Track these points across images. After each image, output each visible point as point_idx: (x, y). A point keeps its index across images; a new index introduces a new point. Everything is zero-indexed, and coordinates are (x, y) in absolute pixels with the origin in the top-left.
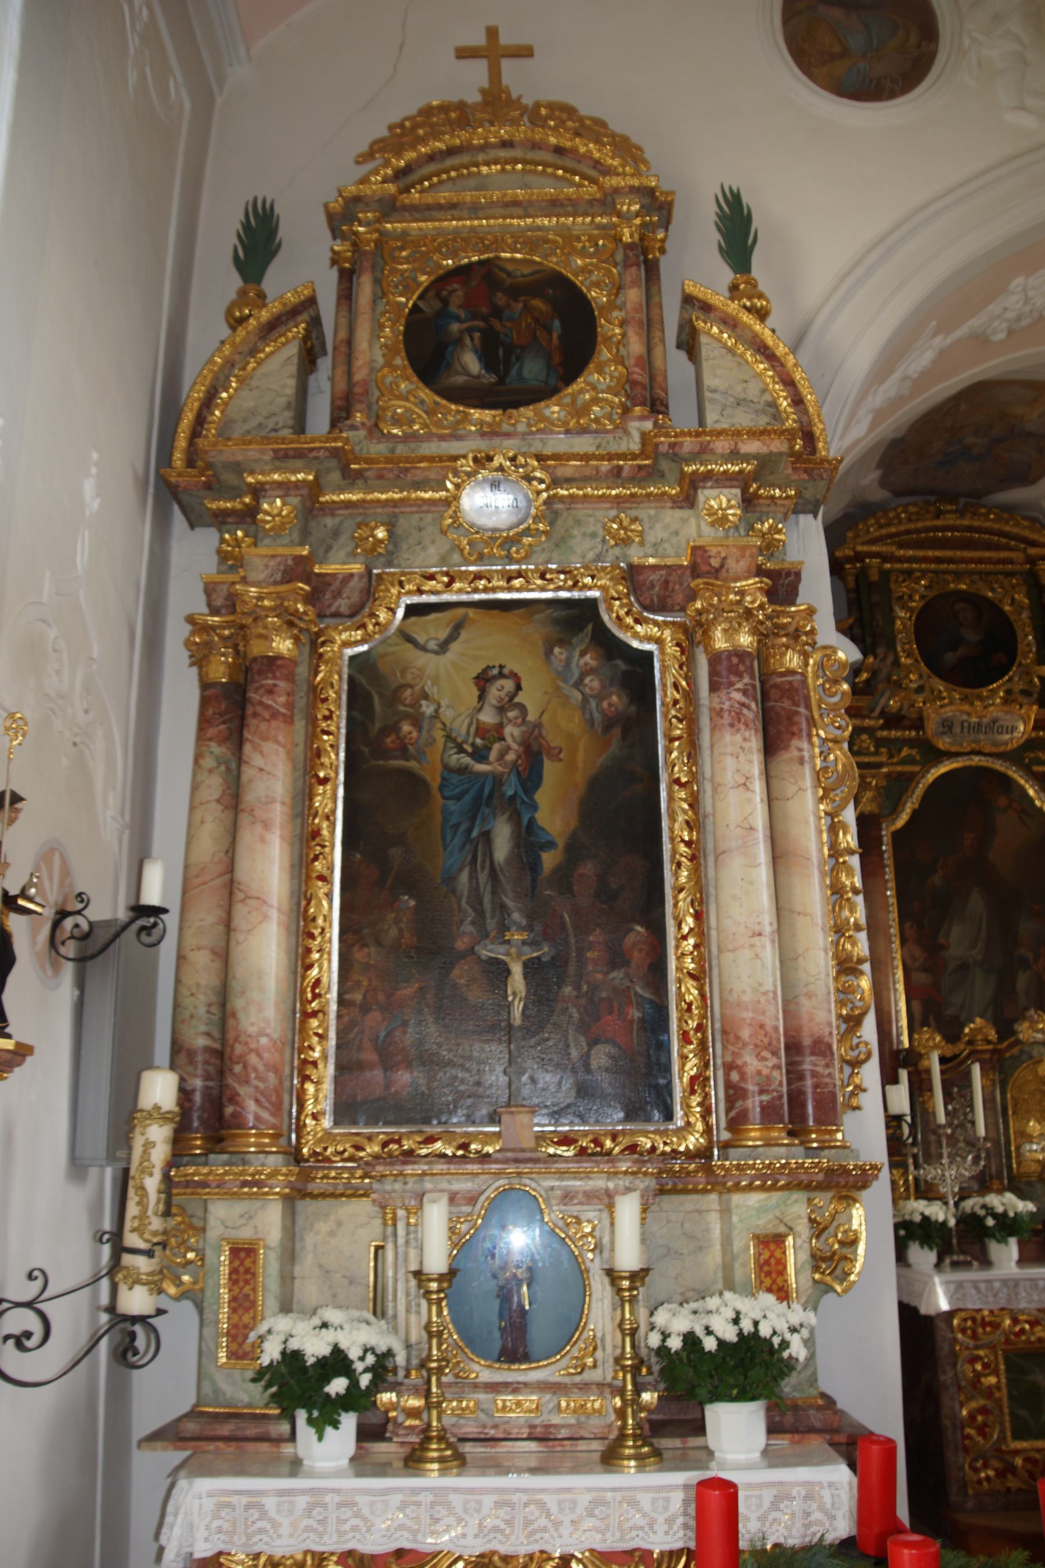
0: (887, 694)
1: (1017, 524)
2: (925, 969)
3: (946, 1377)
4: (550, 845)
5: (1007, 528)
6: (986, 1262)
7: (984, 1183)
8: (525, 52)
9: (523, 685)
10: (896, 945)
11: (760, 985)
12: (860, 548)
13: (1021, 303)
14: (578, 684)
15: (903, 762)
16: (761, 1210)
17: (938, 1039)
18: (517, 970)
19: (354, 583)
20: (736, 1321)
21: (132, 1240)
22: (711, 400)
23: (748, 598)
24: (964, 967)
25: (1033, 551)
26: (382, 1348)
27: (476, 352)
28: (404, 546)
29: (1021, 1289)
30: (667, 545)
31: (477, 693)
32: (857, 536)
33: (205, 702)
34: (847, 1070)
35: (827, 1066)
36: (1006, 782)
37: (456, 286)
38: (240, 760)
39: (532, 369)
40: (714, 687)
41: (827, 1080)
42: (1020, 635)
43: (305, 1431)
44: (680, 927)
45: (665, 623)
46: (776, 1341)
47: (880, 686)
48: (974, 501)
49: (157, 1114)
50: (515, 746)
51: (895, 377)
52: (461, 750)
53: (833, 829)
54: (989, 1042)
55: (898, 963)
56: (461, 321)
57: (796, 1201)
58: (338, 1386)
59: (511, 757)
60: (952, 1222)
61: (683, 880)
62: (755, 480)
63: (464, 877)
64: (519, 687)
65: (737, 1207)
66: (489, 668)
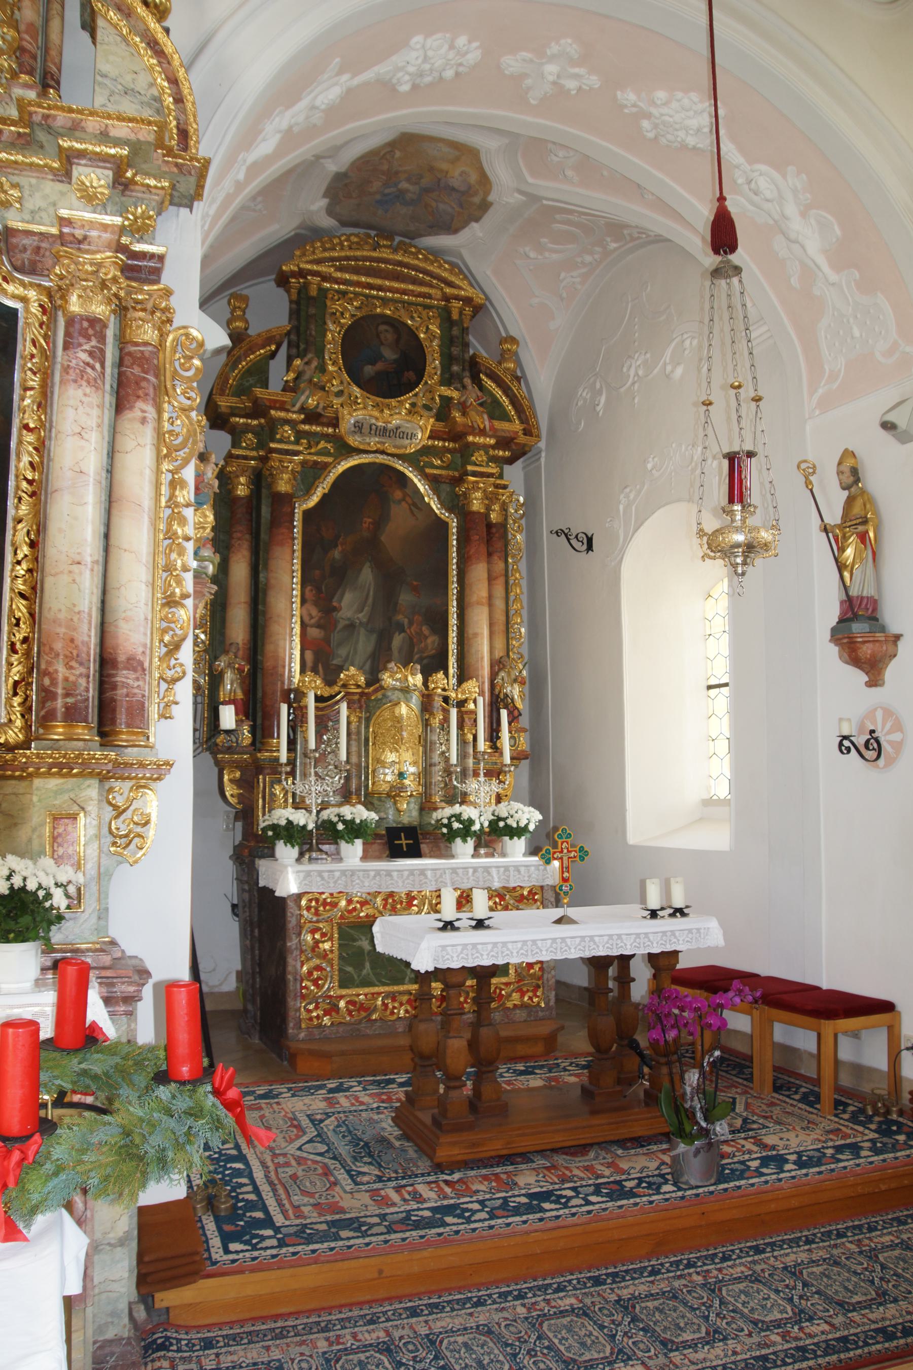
0: (307, 393)
1: (440, 266)
2: (319, 626)
3: (292, 943)
5: (430, 268)
6: (337, 857)
7: (346, 796)
10: (296, 606)
11: (74, 605)
12: (302, 266)
13: (420, 61)
15: (317, 454)
16: (58, 792)
17: (318, 682)
20: (9, 878)
23: (103, 270)
24: (351, 627)
25: (448, 290)
29: (355, 877)
30: (44, 214)
32: (304, 255)
34: (164, 686)
35: (137, 679)
36: (403, 479)
40: (66, 347)
41: (136, 691)
42: (429, 358)
44: (15, 553)
45: (31, 285)
46: (41, 893)
47: (302, 385)
48: (407, 241)
51: (302, 104)
53: (173, 484)
54: (358, 686)
55: (296, 620)
57: (89, 786)
60: (311, 826)
61: (21, 513)
62: (129, 166)
65: (37, 789)
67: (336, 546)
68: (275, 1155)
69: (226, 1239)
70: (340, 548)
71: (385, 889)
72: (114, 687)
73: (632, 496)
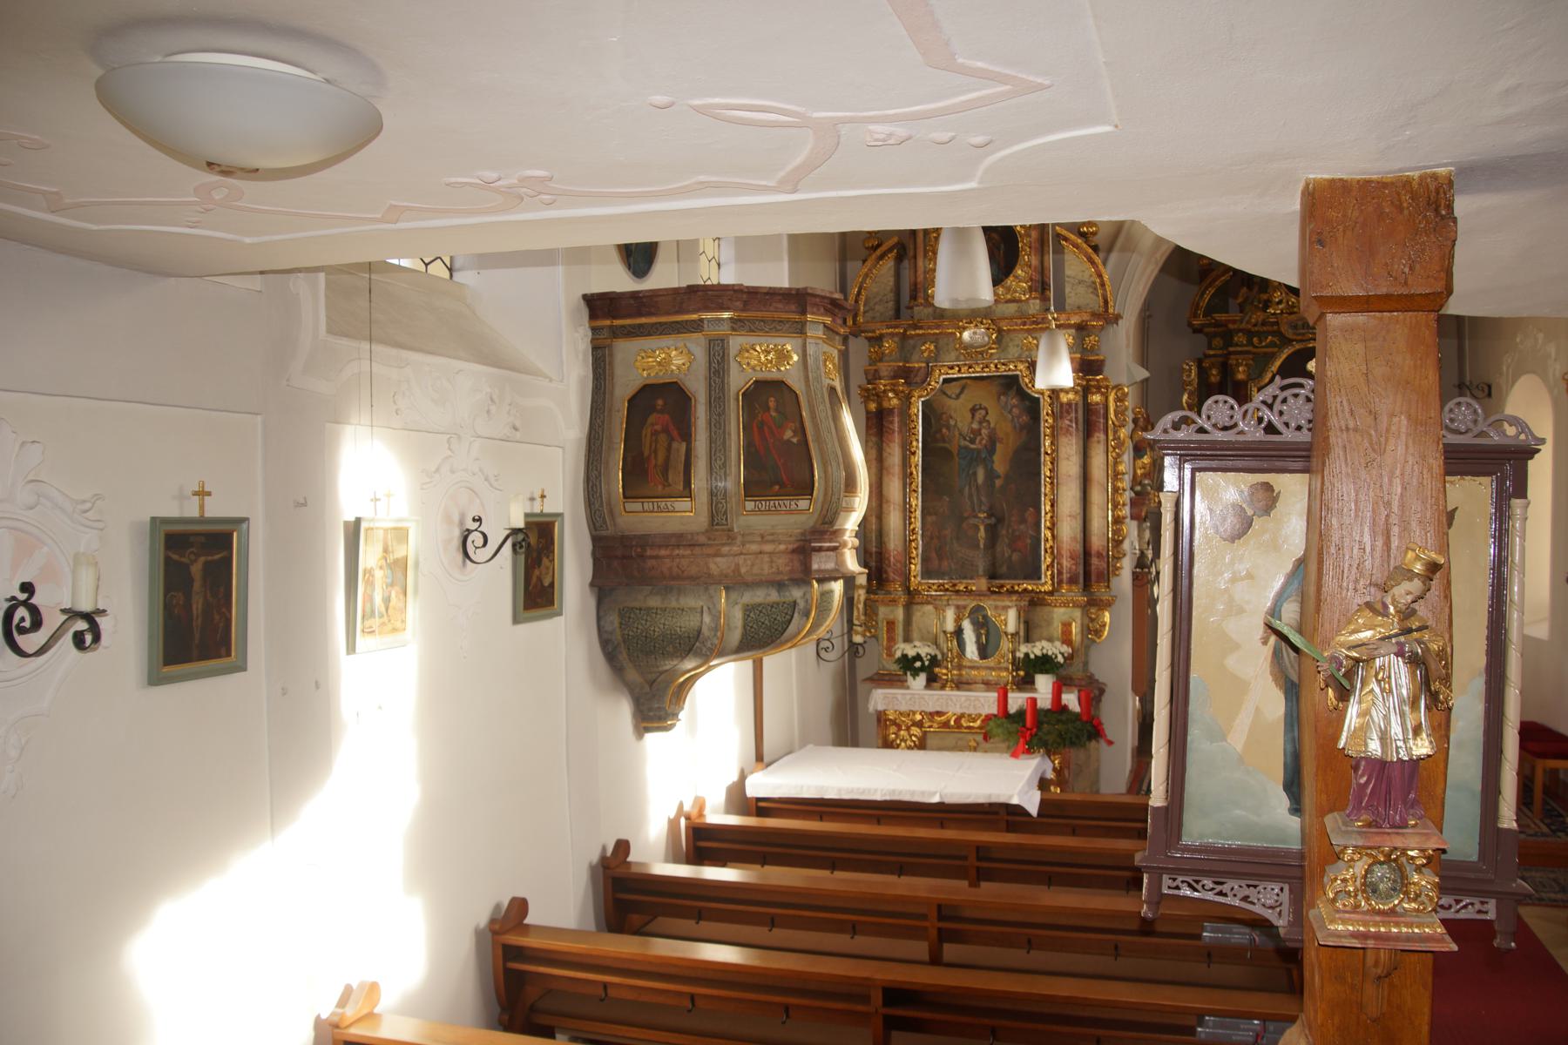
4: (998, 477)
9: (989, 412)
14: (1010, 412)
15: (1266, 346)
16: (1064, 614)
18: (982, 528)
19: (922, 370)
20: (1042, 650)
21: (856, 622)
22: (1068, 282)
26: (933, 654)
28: (941, 352)
31: (970, 416)
33: (868, 419)
38: (882, 441)
43: (910, 678)
46: (1054, 656)
49: (861, 587)
50: (986, 438)
52: (965, 439)
58: (918, 664)
59: (984, 442)
64: (987, 413)
66: (976, 405)
72: (1090, 565)
73: (1509, 361)
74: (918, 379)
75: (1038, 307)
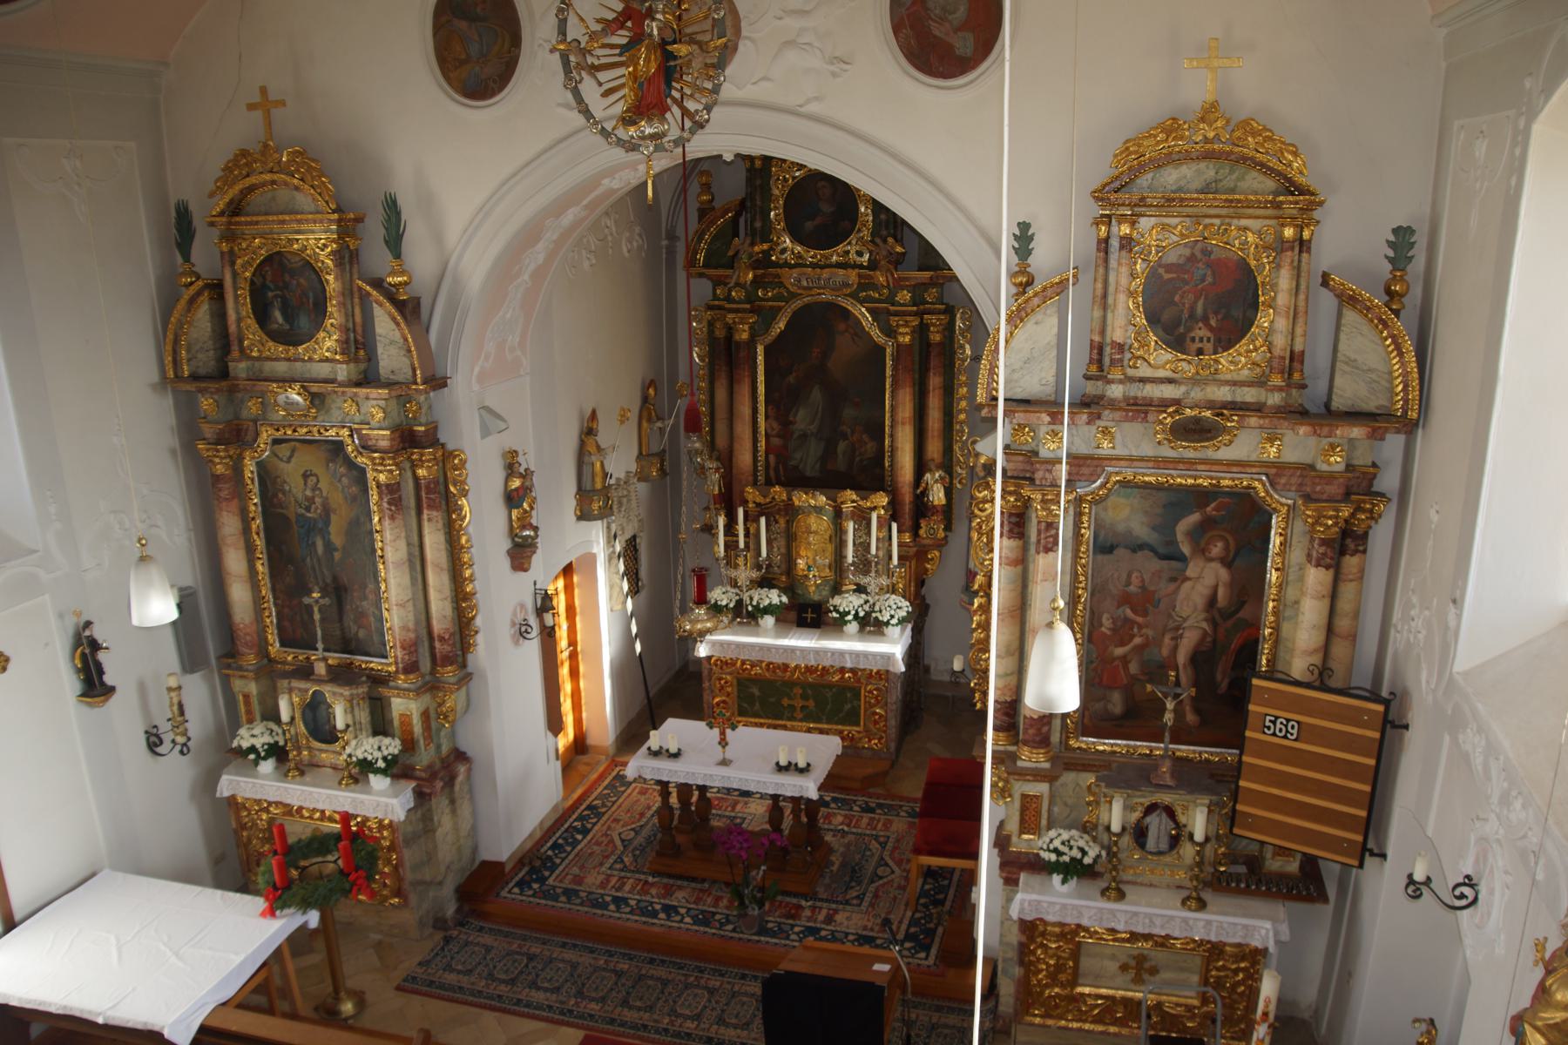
2: (778, 436)
8: (283, 103)
14: (340, 481)
24: (804, 436)
26: (272, 741)
27: (280, 310)
36: (846, 314)
37: (267, 268)
39: (304, 322)
56: (272, 291)
59: (319, 511)
63: (308, 559)
64: (318, 481)
67: (791, 373)
68: (606, 835)
69: (519, 884)
70: (794, 374)
71: (767, 660)
74: (249, 438)
75: (345, 373)
